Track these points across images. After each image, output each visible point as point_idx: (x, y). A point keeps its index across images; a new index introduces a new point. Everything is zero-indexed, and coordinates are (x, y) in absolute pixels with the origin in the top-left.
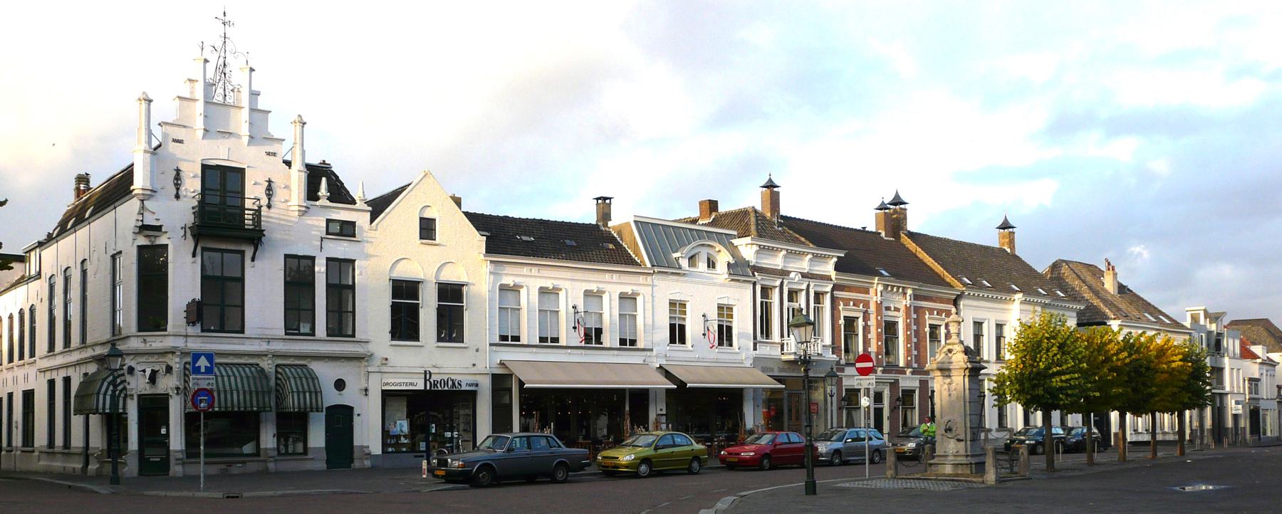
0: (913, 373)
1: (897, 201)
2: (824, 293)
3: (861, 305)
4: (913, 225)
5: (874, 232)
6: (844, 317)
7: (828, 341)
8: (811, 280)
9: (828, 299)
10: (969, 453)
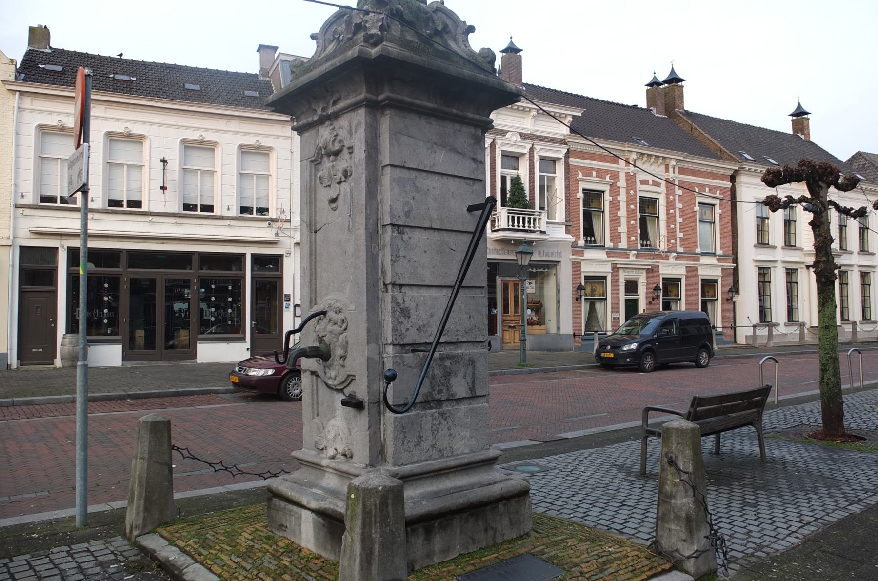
0: (677, 258)
1: (674, 80)
2: (554, 161)
3: (608, 177)
4: (690, 105)
5: (645, 109)
6: (584, 190)
7: (560, 215)
8: (536, 142)
9: (560, 169)
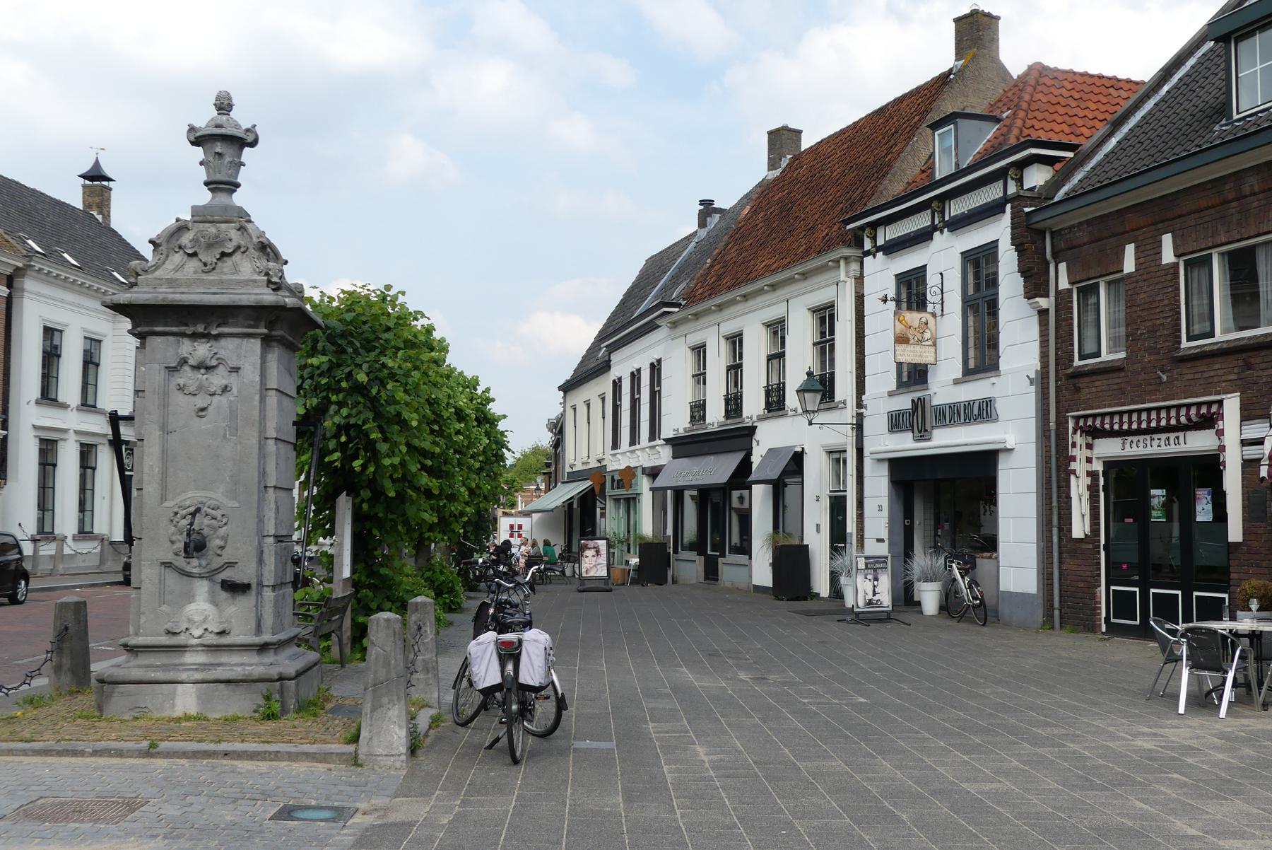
10: (267, 637)
